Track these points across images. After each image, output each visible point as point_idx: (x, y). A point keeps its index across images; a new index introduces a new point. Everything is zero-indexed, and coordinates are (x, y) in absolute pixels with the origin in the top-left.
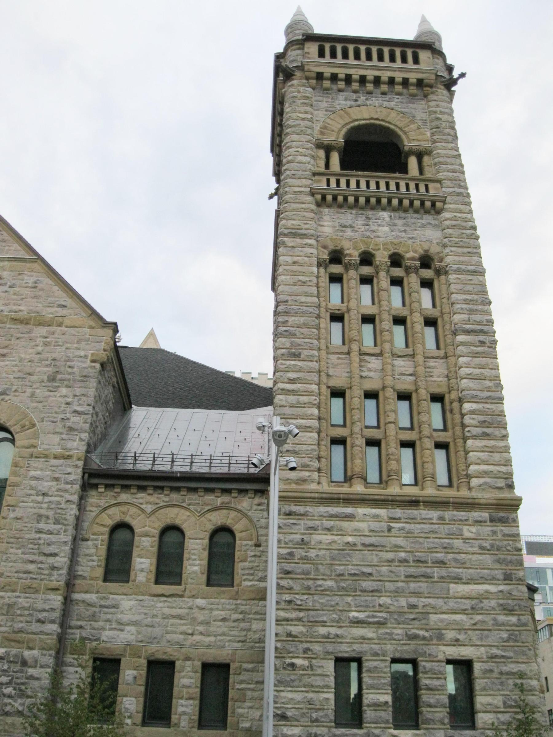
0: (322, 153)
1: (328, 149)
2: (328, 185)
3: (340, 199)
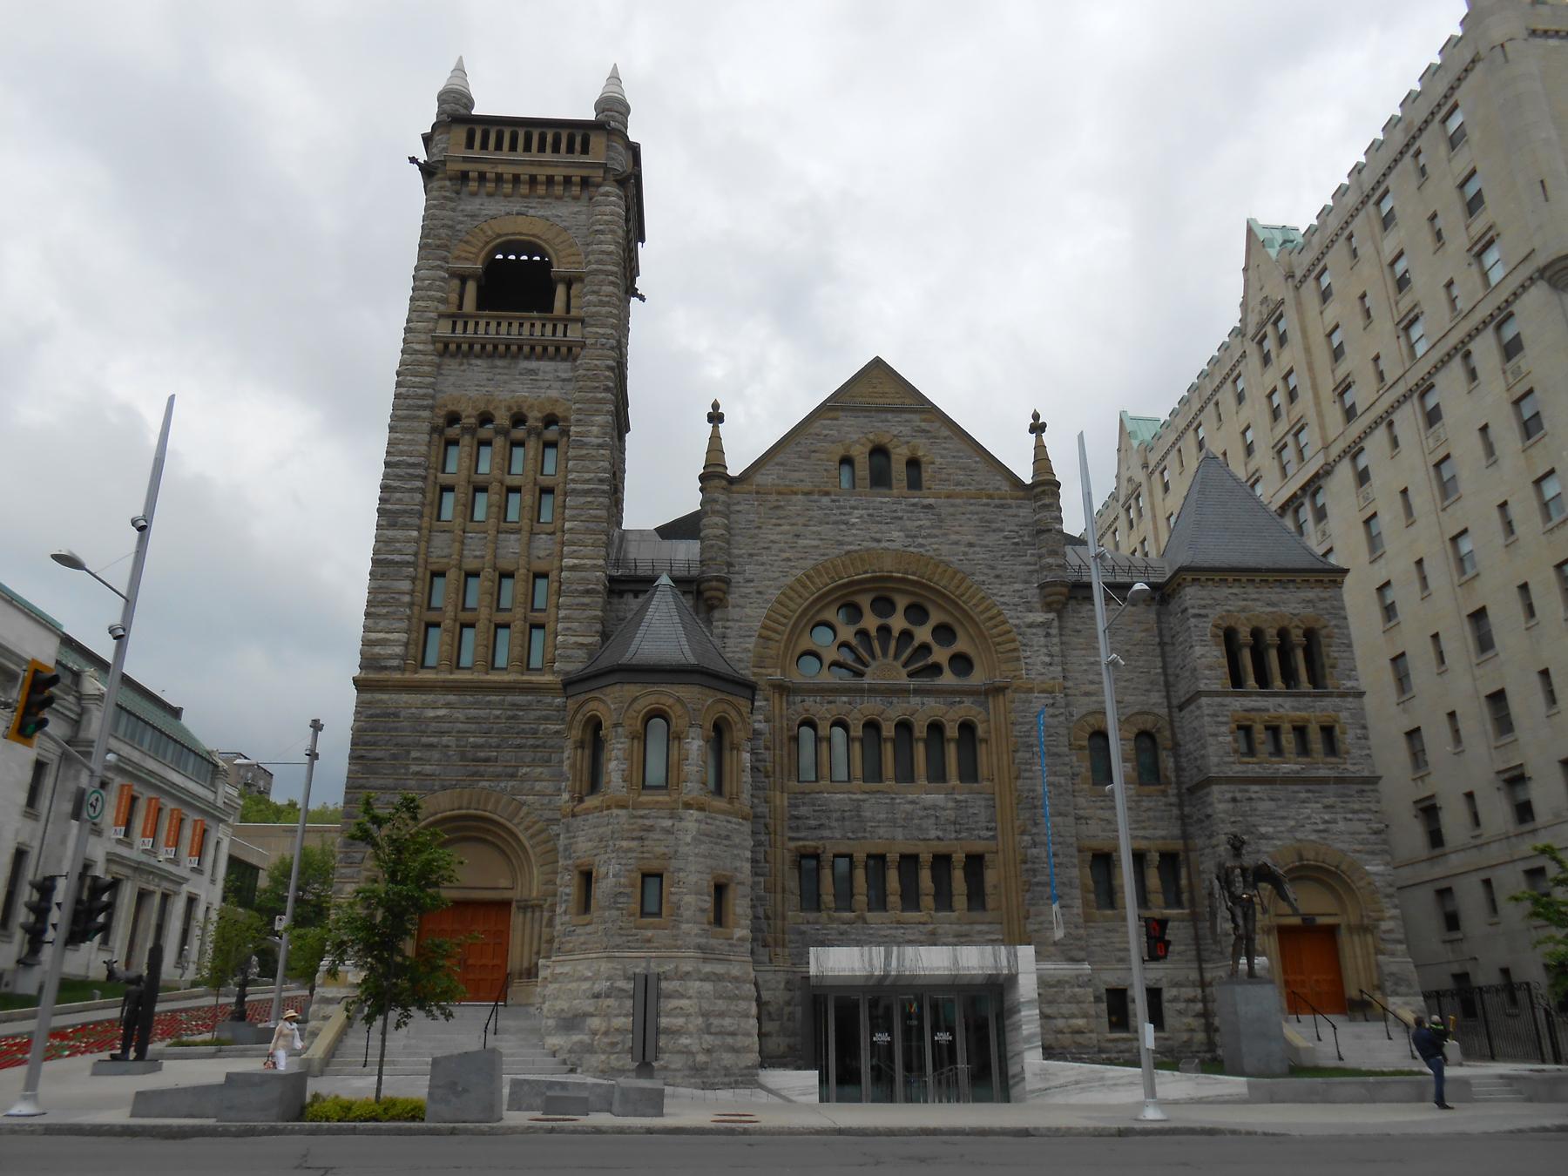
0: (456, 283)
1: (463, 279)
2: (454, 331)
3: (465, 347)
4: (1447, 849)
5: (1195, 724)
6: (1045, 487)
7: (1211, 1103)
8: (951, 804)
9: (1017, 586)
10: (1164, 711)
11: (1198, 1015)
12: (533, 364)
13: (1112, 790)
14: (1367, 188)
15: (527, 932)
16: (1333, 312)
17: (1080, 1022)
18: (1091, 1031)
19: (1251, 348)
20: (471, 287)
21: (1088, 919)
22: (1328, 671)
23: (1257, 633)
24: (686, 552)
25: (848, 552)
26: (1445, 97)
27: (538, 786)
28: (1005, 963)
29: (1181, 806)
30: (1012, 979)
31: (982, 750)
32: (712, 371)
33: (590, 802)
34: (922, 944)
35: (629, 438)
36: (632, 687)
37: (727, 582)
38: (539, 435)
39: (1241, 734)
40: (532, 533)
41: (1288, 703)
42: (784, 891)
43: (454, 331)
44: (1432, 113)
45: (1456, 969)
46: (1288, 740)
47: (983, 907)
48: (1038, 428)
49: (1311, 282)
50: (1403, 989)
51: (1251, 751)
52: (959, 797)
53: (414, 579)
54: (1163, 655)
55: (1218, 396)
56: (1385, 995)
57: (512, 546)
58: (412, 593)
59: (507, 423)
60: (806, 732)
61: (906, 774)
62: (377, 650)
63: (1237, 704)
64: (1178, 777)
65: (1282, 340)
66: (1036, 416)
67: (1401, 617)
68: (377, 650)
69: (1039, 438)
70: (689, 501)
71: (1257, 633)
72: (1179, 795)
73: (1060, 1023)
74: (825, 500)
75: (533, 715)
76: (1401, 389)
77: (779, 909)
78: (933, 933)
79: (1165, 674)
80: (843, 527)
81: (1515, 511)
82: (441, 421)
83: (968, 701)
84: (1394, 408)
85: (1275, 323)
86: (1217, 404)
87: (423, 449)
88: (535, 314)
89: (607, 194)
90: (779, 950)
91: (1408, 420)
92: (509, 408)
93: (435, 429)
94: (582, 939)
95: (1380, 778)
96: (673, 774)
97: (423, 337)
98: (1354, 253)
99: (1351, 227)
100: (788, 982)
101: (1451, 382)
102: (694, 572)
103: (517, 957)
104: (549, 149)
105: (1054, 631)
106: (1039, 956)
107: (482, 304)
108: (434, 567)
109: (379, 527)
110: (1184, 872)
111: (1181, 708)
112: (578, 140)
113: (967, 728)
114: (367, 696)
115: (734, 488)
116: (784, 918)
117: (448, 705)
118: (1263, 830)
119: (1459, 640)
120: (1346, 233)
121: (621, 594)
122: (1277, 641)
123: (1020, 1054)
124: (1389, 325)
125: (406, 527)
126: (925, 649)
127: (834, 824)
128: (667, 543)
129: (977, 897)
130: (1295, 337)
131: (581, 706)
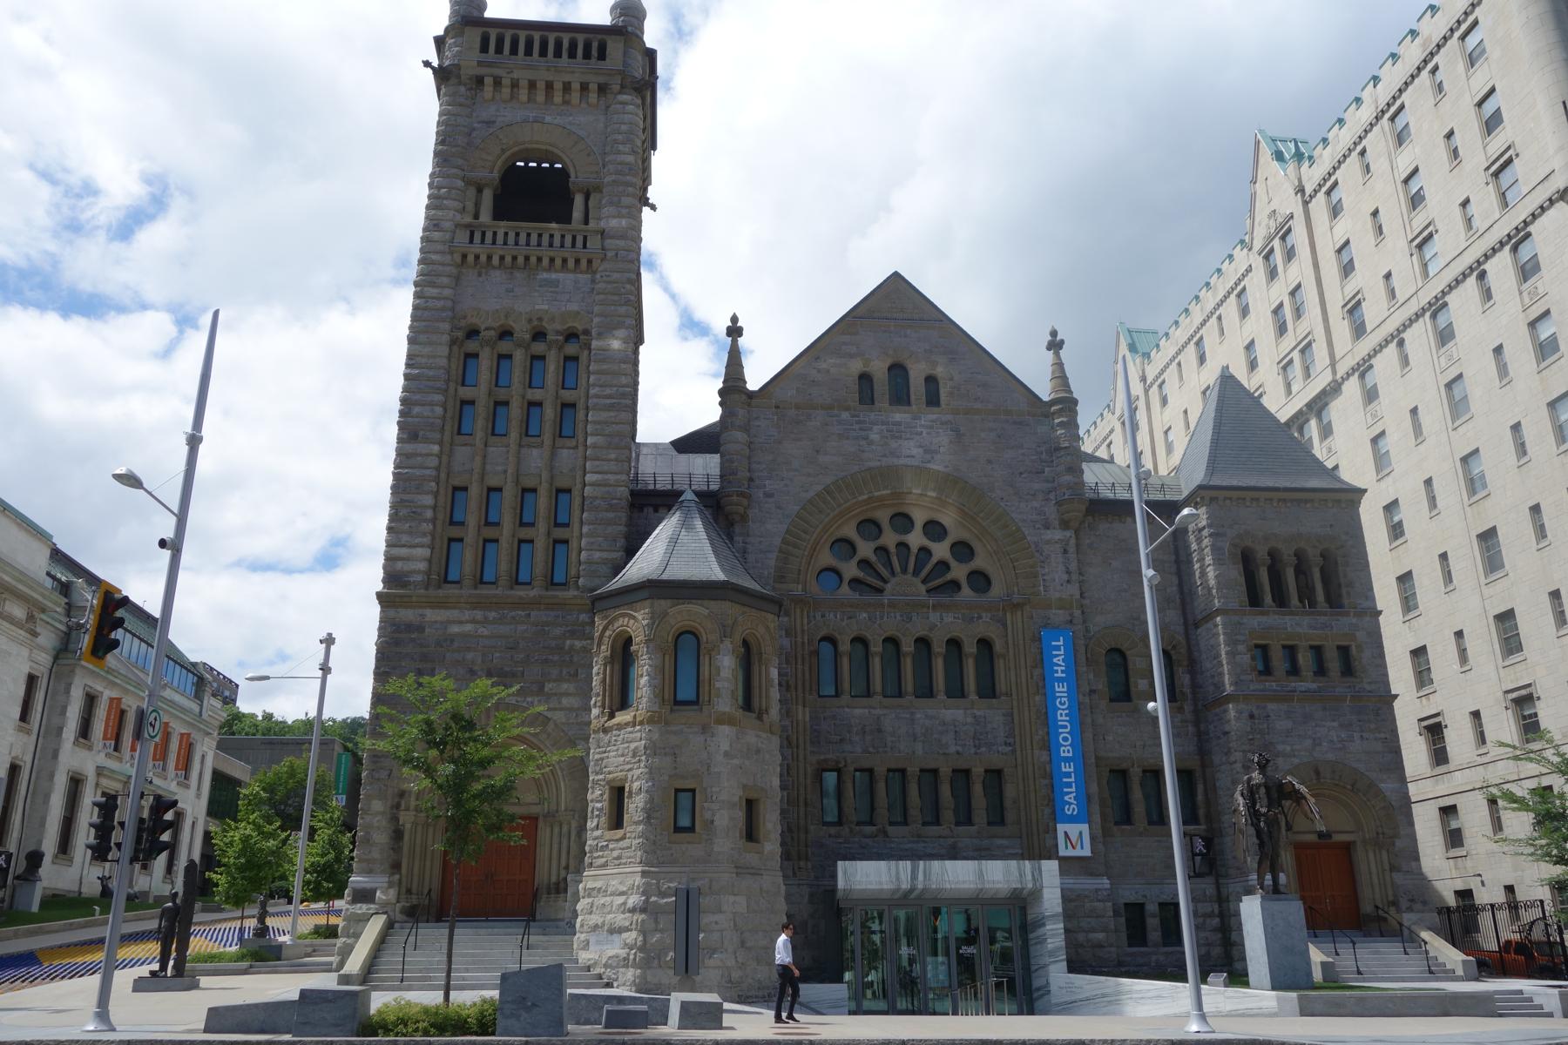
0: (472, 192)
1: (480, 191)
2: (471, 241)
4: (1452, 766)
5: (1212, 642)
6: (1067, 404)
7: (1243, 1015)
8: (969, 720)
9: (1035, 504)
10: (1181, 629)
11: (1215, 930)
12: (554, 276)
13: (1156, 710)
14: (1382, 104)
15: (555, 846)
16: (1343, 229)
17: (1101, 936)
18: (1111, 946)
19: (1258, 262)
20: (488, 195)
21: (1106, 833)
22: (1344, 591)
23: (1273, 554)
24: (706, 467)
25: (870, 469)
26: (1465, 13)
27: (565, 701)
28: (1029, 877)
29: (1197, 723)
30: (1036, 894)
31: (1000, 665)
32: (726, 283)
33: (622, 717)
34: (942, 857)
35: (642, 348)
36: (663, 602)
37: (748, 497)
38: (560, 348)
39: (1258, 652)
40: (554, 446)
41: (1306, 620)
42: (806, 804)
43: (471, 241)
44: (1452, 30)
45: (1460, 886)
46: (1305, 659)
47: (1002, 822)
48: (1055, 345)
49: (1321, 195)
50: (1418, 906)
51: (1267, 671)
52: (978, 713)
53: (436, 495)
54: (1179, 574)
55: (1221, 310)
56: (1399, 910)
57: (535, 459)
58: (435, 508)
59: (528, 337)
60: (826, 648)
61: (926, 691)
62: (399, 565)
63: (1255, 621)
64: (1194, 693)
65: (1290, 254)
66: (1054, 333)
67: (1408, 535)
68: (399, 565)
69: (1057, 355)
70: (705, 411)
71: (1273, 554)
72: (1196, 712)
73: (1081, 937)
74: (845, 415)
75: (558, 631)
76: (1413, 307)
77: (802, 822)
78: (954, 847)
79: (1181, 592)
80: (863, 443)
81: (1528, 433)
82: (460, 334)
83: (986, 617)
84: (1405, 327)
85: (1283, 238)
86: (1219, 318)
87: (444, 362)
88: (554, 225)
89: (624, 103)
90: (802, 864)
91: (1420, 337)
92: (530, 321)
93: (453, 342)
94: (615, 854)
95: (1396, 696)
96: (705, 689)
97: (440, 247)
98: (1368, 168)
99: (1364, 142)
100: (811, 895)
101: (1465, 300)
102: (714, 487)
103: (545, 871)
104: (565, 54)
105: (1072, 549)
106: (1063, 872)
107: (498, 215)
108: (457, 483)
109: (400, 440)
110: (1200, 788)
111: (1197, 626)
112: (595, 45)
113: (985, 644)
114: (392, 613)
115: (754, 402)
116: (807, 832)
117: (473, 621)
118: (1280, 747)
119: (1466, 561)
120: (1359, 148)
121: (641, 508)
122: (1294, 560)
123: (1045, 966)
124: (1402, 244)
125: (427, 441)
126: (943, 565)
127: (856, 738)
128: (684, 457)
129: (997, 817)
130: (1303, 251)
131: (610, 623)
